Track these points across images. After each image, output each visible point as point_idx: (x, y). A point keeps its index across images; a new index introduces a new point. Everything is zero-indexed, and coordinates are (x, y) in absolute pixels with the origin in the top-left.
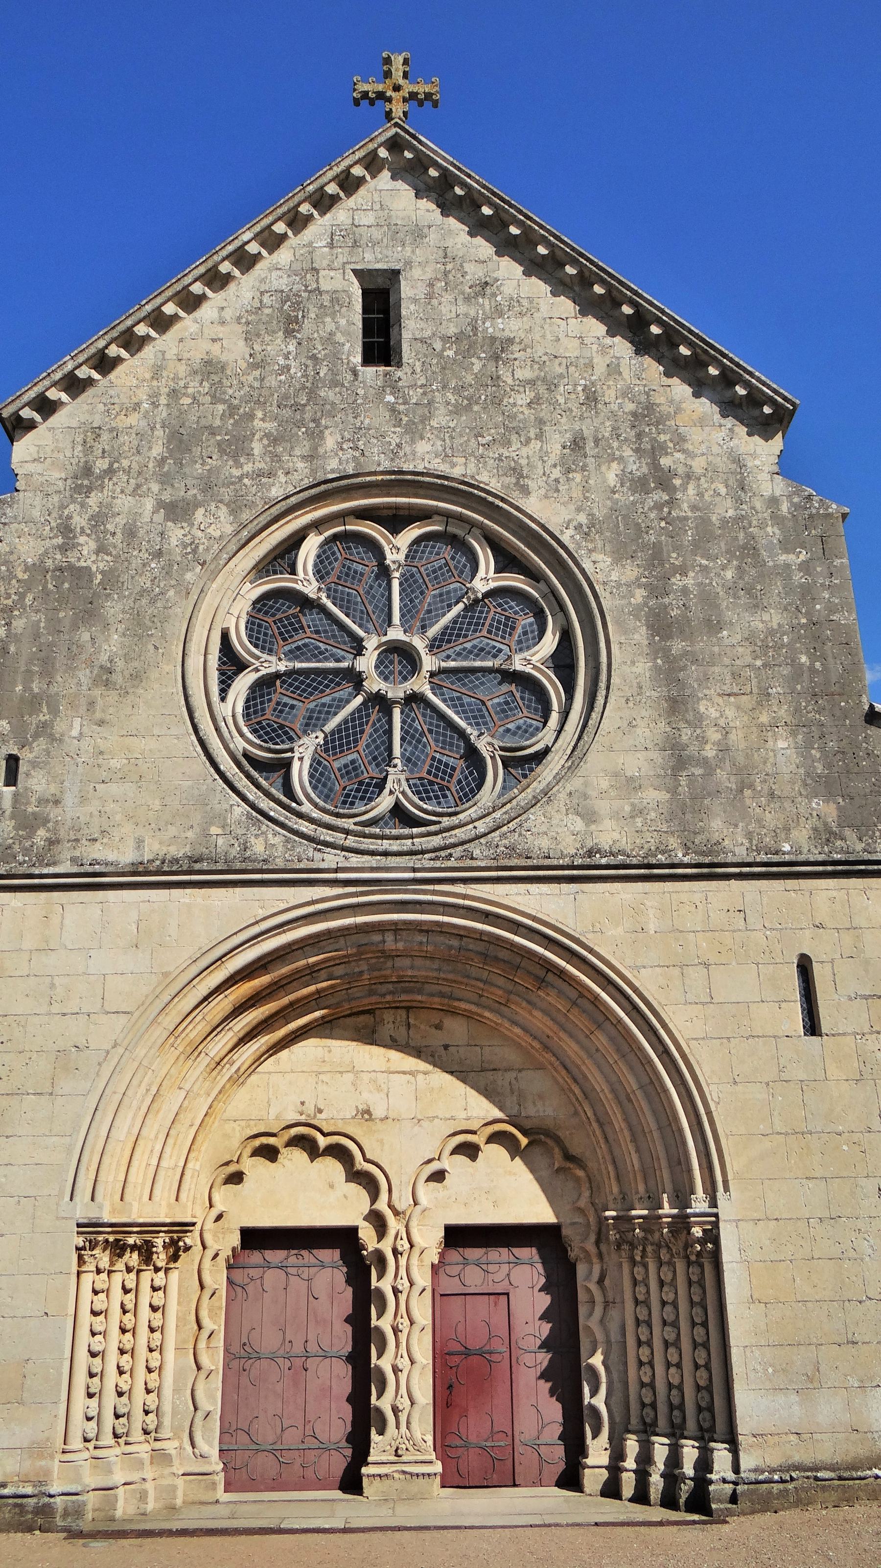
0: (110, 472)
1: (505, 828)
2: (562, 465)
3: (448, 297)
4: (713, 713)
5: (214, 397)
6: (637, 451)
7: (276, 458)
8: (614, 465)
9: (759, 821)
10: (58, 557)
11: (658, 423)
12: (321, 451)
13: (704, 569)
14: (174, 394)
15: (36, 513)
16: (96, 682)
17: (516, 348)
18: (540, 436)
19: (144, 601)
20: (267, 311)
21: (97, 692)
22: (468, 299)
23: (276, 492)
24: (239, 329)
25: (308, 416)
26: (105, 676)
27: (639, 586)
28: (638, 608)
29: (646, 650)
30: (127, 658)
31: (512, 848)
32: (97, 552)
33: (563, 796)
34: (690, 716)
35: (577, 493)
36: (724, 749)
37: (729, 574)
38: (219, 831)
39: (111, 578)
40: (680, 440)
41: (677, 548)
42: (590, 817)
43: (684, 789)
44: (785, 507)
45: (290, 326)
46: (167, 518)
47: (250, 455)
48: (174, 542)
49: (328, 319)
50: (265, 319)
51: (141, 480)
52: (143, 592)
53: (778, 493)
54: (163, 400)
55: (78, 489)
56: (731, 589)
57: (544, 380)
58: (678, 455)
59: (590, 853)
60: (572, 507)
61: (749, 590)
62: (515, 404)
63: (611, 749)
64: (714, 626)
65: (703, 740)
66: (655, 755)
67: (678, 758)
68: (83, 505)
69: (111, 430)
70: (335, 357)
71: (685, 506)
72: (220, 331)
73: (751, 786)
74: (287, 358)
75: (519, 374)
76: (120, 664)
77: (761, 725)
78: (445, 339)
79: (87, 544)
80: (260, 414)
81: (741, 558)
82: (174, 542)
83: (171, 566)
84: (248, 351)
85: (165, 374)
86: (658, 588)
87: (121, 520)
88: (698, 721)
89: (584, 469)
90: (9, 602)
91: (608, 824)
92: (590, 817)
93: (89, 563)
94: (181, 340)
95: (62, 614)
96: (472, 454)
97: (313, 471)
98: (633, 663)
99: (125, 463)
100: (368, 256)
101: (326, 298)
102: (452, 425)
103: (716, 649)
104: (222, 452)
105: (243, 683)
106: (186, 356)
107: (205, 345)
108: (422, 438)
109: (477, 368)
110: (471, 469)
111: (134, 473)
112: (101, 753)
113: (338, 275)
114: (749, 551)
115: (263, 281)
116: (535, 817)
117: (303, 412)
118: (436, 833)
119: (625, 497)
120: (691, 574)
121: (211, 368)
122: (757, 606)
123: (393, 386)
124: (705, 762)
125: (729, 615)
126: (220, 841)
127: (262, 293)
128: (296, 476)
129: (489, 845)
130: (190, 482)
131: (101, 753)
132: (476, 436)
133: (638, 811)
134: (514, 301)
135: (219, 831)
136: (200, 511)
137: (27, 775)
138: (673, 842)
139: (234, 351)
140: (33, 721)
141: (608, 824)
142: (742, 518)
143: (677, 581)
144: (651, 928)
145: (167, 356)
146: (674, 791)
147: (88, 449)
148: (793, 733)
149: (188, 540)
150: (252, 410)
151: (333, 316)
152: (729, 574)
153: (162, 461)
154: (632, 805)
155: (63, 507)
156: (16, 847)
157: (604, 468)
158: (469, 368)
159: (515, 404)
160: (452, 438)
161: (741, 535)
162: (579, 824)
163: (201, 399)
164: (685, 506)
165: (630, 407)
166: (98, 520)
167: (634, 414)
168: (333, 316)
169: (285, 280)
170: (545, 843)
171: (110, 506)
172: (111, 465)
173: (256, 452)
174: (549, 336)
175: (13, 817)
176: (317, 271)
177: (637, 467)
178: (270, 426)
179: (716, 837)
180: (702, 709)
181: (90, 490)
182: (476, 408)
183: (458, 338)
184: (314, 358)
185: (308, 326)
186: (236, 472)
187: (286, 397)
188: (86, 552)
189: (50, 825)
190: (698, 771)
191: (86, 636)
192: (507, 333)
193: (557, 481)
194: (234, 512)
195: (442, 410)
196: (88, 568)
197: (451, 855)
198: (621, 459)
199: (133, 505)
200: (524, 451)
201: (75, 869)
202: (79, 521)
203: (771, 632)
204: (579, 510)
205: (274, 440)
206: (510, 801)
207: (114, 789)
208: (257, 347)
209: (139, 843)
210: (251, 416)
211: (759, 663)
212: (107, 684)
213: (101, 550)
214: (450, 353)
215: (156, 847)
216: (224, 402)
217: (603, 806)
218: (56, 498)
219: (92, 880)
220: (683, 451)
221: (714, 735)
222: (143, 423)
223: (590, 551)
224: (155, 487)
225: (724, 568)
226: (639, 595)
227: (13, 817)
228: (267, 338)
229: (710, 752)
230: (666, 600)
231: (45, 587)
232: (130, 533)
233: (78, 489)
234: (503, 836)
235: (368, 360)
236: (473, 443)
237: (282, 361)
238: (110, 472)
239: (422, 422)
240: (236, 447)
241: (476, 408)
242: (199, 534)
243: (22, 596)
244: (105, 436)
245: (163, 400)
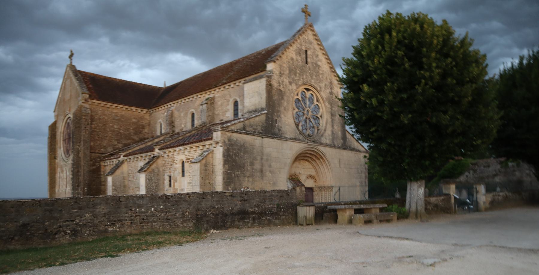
166: (283, 82)
202: (281, 82)
213: (283, 87)
219: (286, 139)
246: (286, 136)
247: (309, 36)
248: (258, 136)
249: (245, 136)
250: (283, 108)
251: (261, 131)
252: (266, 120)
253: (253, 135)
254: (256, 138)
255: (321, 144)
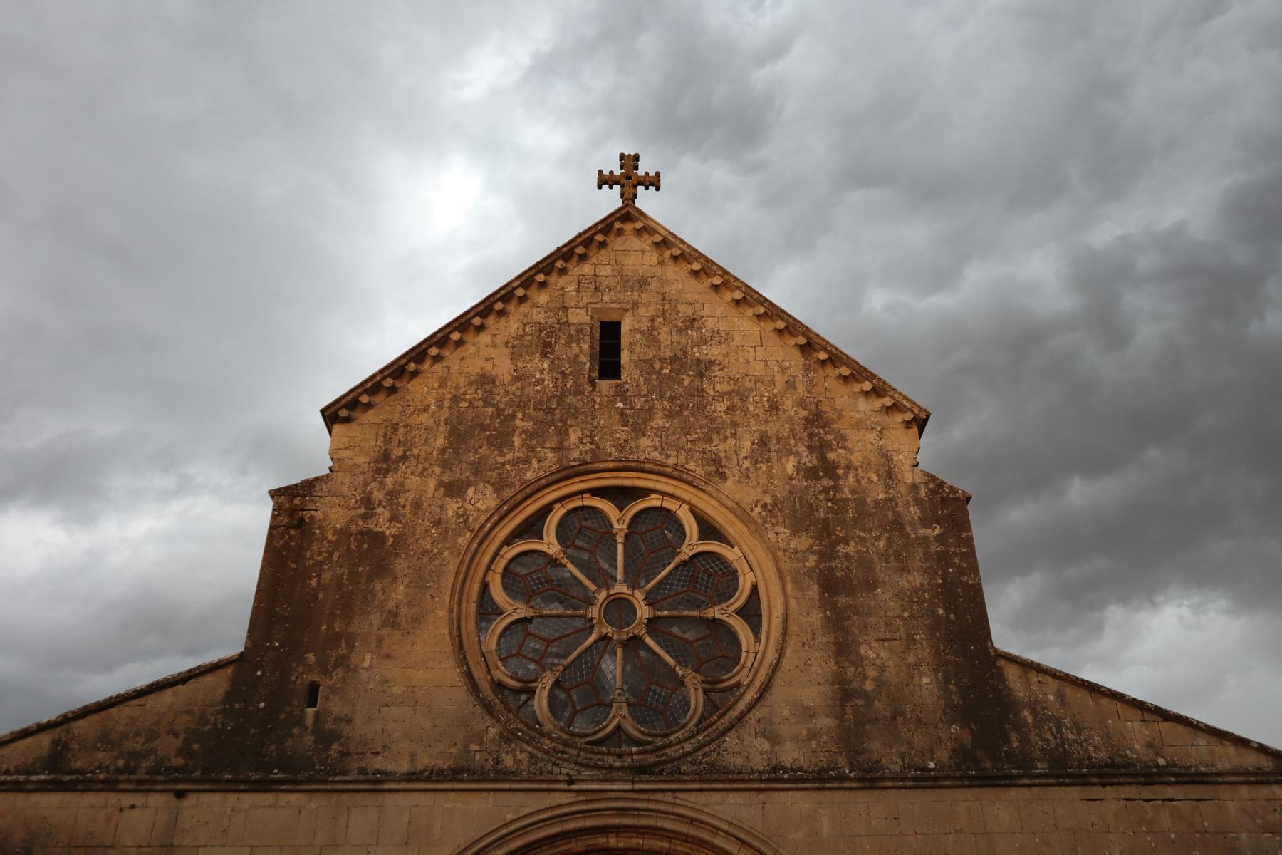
0: (404, 458)
1: (707, 749)
2: (752, 457)
3: (665, 330)
4: (871, 655)
5: (485, 402)
6: (809, 447)
7: (531, 449)
8: (792, 458)
9: (910, 743)
10: (360, 523)
11: (824, 427)
12: (566, 444)
13: (862, 539)
14: (455, 399)
15: (345, 489)
16: (384, 624)
17: (716, 368)
18: (734, 435)
19: (425, 560)
20: (528, 338)
21: (384, 632)
22: (680, 331)
23: (530, 475)
24: (507, 351)
25: (557, 417)
26: (392, 620)
27: (812, 553)
28: (812, 570)
29: (818, 604)
30: (409, 604)
31: (712, 765)
32: (390, 520)
33: (753, 722)
34: (853, 658)
35: (763, 480)
36: (880, 683)
37: (882, 544)
38: (477, 748)
39: (400, 540)
40: (843, 438)
41: (842, 523)
42: (774, 740)
43: (849, 716)
44: (923, 492)
45: (546, 349)
46: (445, 495)
47: (512, 446)
48: (450, 513)
49: (574, 345)
50: (526, 343)
51: (427, 465)
52: (425, 552)
53: (917, 481)
54: (447, 404)
55: (378, 471)
56: (884, 556)
57: (738, 392)
58: (840, 451)
59: (775, 769)
60: (760, 490)
61: (898, 557)
62: (715, 411)
63: (791, 684)
64: (871, 585)
65: (864, 677)
66: (826, 689)
67: (844, 692)
68: (381, 483)
69: (406, 426)
70: (578, 373)
71: (847, 490)
72: (491, 352)
73: (902, 714)
74: (542, 372)
75: (718, 388)
76: (404, 610)
77: (909, 665)
78: (662, 360)
79: (383, 514)
80: (520, 415)
81: (892, 530)
82: (450, 513)
83: (447, 532)
84: (513, 367)
85: (449, 384)
86: (827, 554)
87: (410, 495)
88: (858, 661)
89: (768, 460)
90: (320, 558)
91: (789, 745)
92: (774, 740)
93: (384, 528)
94: (463, 359)
95: (361, 569)
96: (683, 448)
97: (560, 460)
98: (808, 614)
99: (416, 451)
100: (606, 298)
101: (573, 330)
102: (667, 425)
103: (873, 603)
104: (490, 444)
105: (500, 624)
106: (466, 370)
107: (481, 363)
108: (644, 435)
109: (686, 383)
110: (682, 459)
111: (421, 460)
112: (386, 681)
113: (583, 312)
114: (897, 525)
115: (526, 315)
116: (730, 740)
117: (553, 414)
118: (651, 752)
119: (800, 483)
120: (852, 543)
121: (485, 380)
122: (904, 570)
123: (621, 393)
124: (866, 695)
125: (882, 576)
126: (478, 756)
127: (525, 325)
128: (547, 464)
129: (693, 763)
130: (464, 466)
131: (386, 681)
132: (685, 435)
133: (813, 735)
134: (714, 334)
135: (477, 748)
136: (472, 489)
137: (327, 698)
138: (841, 761)
139: (503, 367)
140: (334, 654)
141: (789, 745)
142: (891, 500)
143: (842, 549)
144: (825, 832)
145: (452, 370)
146: (841, 718)
147: (388, 440)
148: (935, 671)
149: (461, 511)
150: (515, 412)
151: (578, 341)
152: (882, 544)
153: (443, 451)
154: (809, 730)
155: (366, 484)
156: (315, 759)
157: (784, 460)
158: (681, 382)
159: (715, 411)
160: (667, 436)
161: (890, 513)
162: (766, 745)
163: (477, 403)
164: (847, 490)
165: (803, 413)
166: (392, 495)
167: (806, 419)
168: (578, 341)
169: (543, 315)
170: (738, 761)
171: (402, 484)
172: (405, 452)
173: (516, 444)
174: (741, 360)
175: (313, 732)
176: (565, 308)
177: (809, 460)
178: (528, 425)
179: (875, 756)
180: (862, 652)
181: (387, 471)
182: (686, 413)
183: (674, 359)
184: (563, 373)
185: (559, 349)
186: (501, 460)
187: (540, 402)
188: (382, 521)
189: (343, 740)
190: (860, 702)
191: (378, 587)
192: (710, 357)
193: (748, 469)
194: (498, 491)
195: (660, 414)
196: (383, 533)
197: (663, 770)
198: (797, 454)
199: (421, 484)
200: (721, 447)
201: (361, 778)
202: (378, 496)
203: (916, 590)
204: (765, 492)
205: (530, 435)
206: (711, 726)
207: (393, 710)
208: (520, 365)
209: (413, 757)
210: (513, 417)
211: (906, 615)
212: (394, 625)
214: (667, 371)
215: (426, 760)
216: (493, 405)
217: (784, 731)
218: (361, 478)
220: (844, 448)
221: (872, 673)
222: (431, 421)
223: (773, 525)
224: (438, 470)
225: (877, 539)
226: (812, 559)
227: (313, 732)
228: (528, 358)
229: (869, 686)
230: (833, 564)
231: (349, 547)
232: (417, 505)
233: (378, 471)
234: (705, 755)
235: (602, 376)
236: (683, 440)
237: (538, 375)
238: (404, 458)
239: (645, 423)
240: (501, 441)
241: (686, 413)
242: (471, 507)
243: (331, 554)
244: (401, 430)
245: (447, 404)
246: (380, 763)
247: (633, 254)
248: (143, 787)
249: (54, 799)
250: (375, 618)
251: (179, 761)
252: (230, 697)
253: (110, 786)
254: (128, 799)
255: (722, 777)
